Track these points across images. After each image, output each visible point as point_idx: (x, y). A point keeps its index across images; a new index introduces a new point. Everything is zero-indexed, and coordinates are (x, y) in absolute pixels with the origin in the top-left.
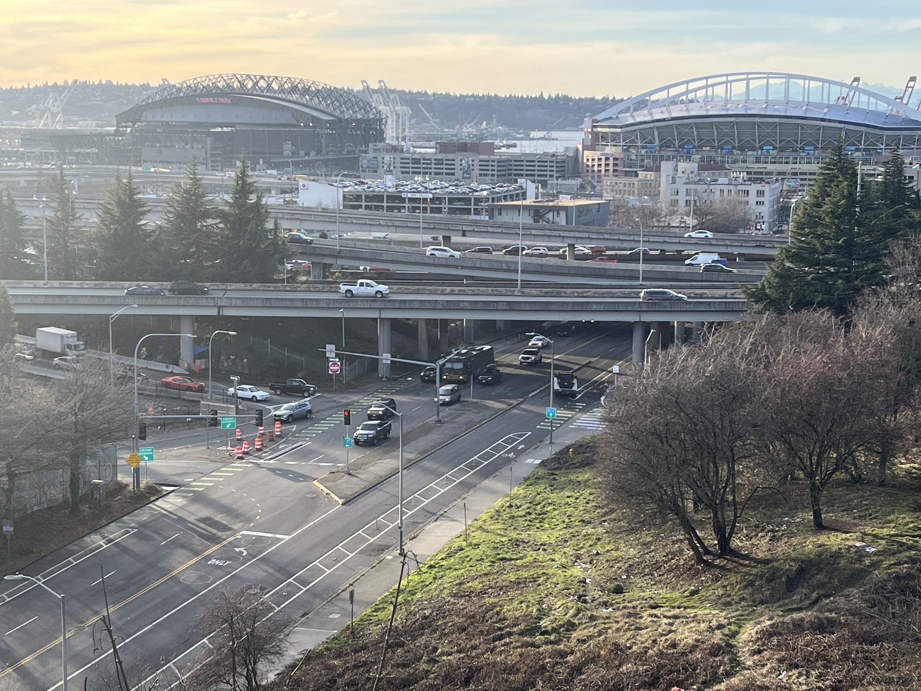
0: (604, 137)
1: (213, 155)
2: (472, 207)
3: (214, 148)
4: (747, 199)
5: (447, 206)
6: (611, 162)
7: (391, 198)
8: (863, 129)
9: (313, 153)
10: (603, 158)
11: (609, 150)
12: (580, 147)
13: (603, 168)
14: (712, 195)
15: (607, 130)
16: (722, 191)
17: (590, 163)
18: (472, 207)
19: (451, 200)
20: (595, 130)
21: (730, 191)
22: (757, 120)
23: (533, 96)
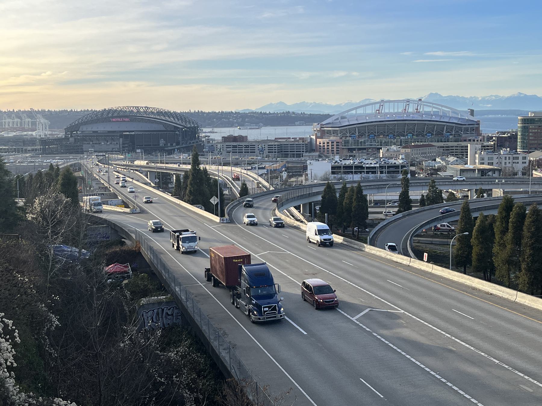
0: (329, 132)
1: (123, 147)
2: (400, 170)
3: (123, 144)
4: (517, 161)
5: (387, 170)
6: (335, 144)
7: (357, 167)
8: (454, 125)
9: (174, 144)
10: (330, 142)
11: (332, 138)
12: (314, 137)
13: (330, 147)
14: (501, 160)
15: (331, 129)
16: (506, 158)
17: (322, 145)
18: (387, 170)
19: (389, 167)
20: (322, 129)
21: (509, 158)
22: (407, 122)
23: (217, 112)
